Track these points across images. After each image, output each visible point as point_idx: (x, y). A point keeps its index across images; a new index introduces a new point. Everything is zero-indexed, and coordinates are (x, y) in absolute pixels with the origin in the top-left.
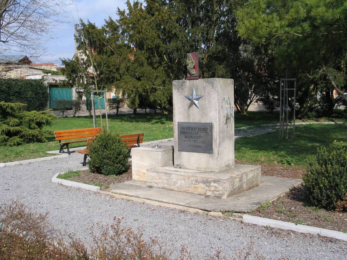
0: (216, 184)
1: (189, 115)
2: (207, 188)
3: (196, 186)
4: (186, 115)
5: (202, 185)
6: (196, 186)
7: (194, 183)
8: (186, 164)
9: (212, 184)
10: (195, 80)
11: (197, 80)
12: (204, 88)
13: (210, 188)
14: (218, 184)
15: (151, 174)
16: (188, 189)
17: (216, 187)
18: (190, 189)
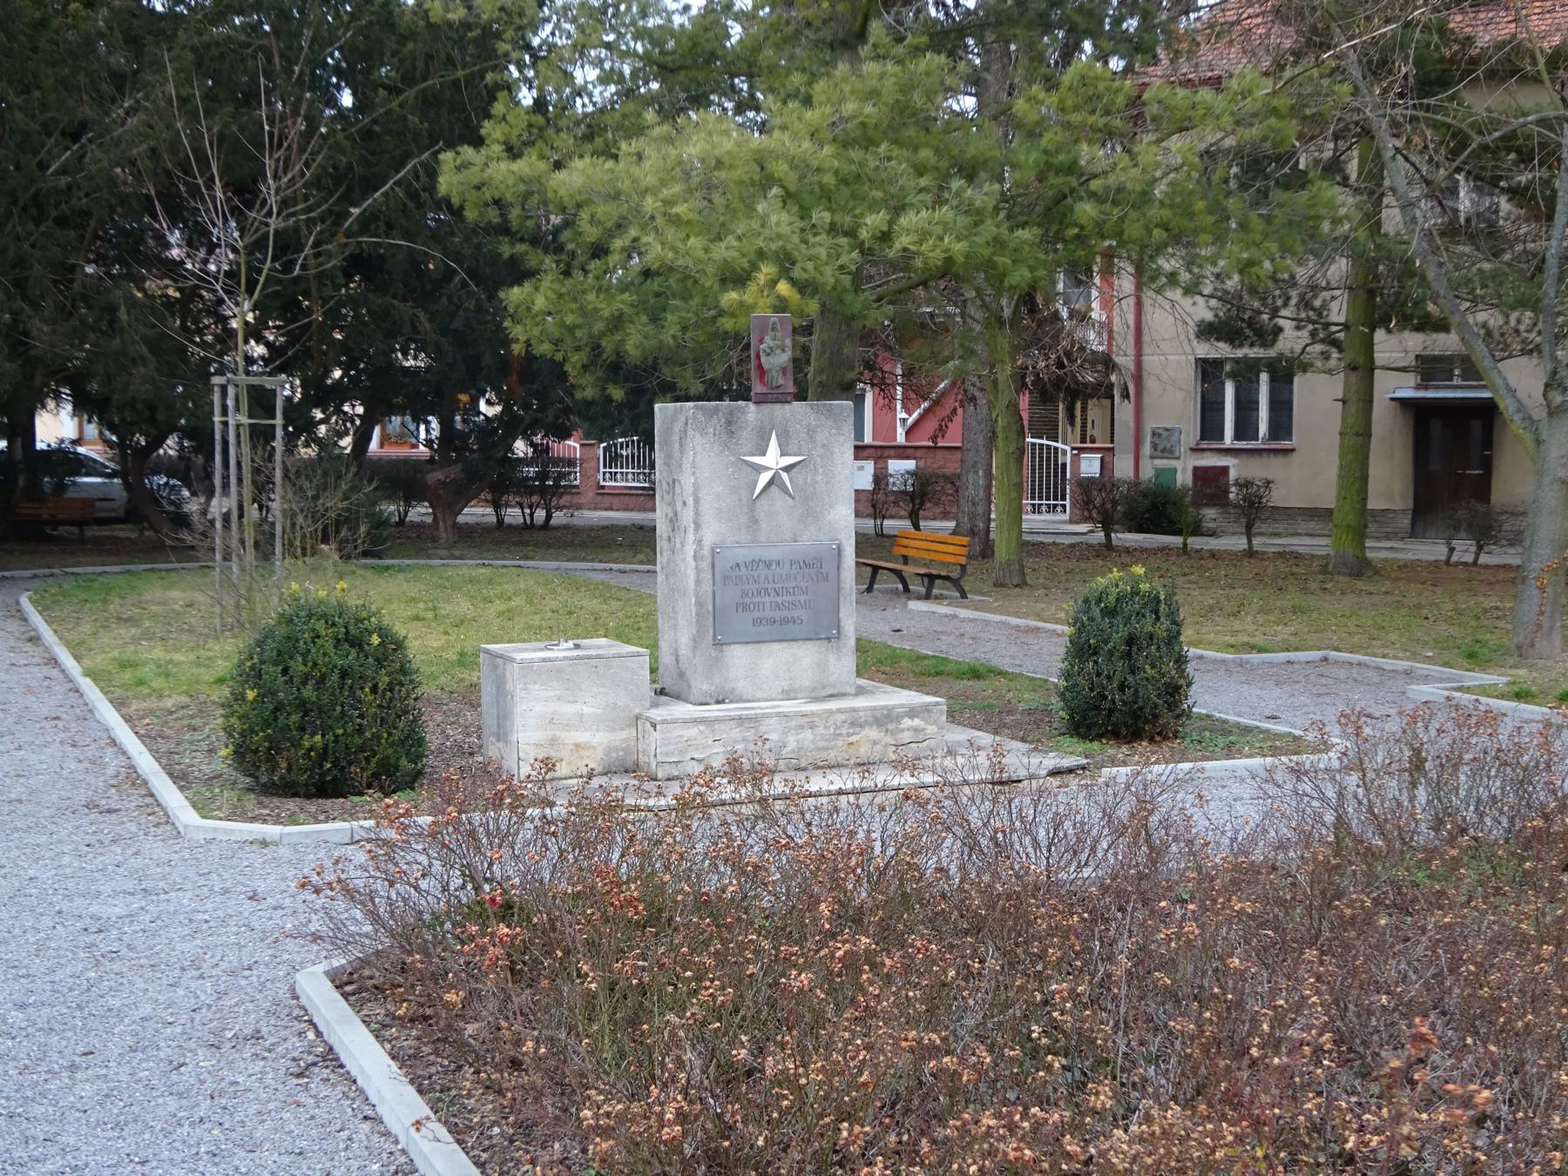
0: (917, 722)
1: (754, 521)
2: (889, 739)
3: (853, 739)
4: (744, 520)
5: (873, 733)
6: (853, 739)
7: (844, 731)
8: (741, 686)
9: (907, 722)
10: (778, 407)
11: (787, 407)
12: (811, 432)
13: (900, 736)
14: (923, 719)
15: (675, 733)
16: (824, 755)
17: (916, 730)
18: (832, 754)
